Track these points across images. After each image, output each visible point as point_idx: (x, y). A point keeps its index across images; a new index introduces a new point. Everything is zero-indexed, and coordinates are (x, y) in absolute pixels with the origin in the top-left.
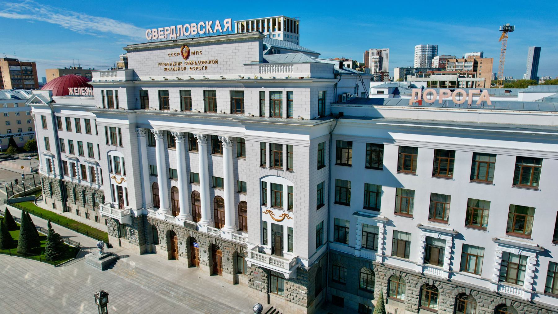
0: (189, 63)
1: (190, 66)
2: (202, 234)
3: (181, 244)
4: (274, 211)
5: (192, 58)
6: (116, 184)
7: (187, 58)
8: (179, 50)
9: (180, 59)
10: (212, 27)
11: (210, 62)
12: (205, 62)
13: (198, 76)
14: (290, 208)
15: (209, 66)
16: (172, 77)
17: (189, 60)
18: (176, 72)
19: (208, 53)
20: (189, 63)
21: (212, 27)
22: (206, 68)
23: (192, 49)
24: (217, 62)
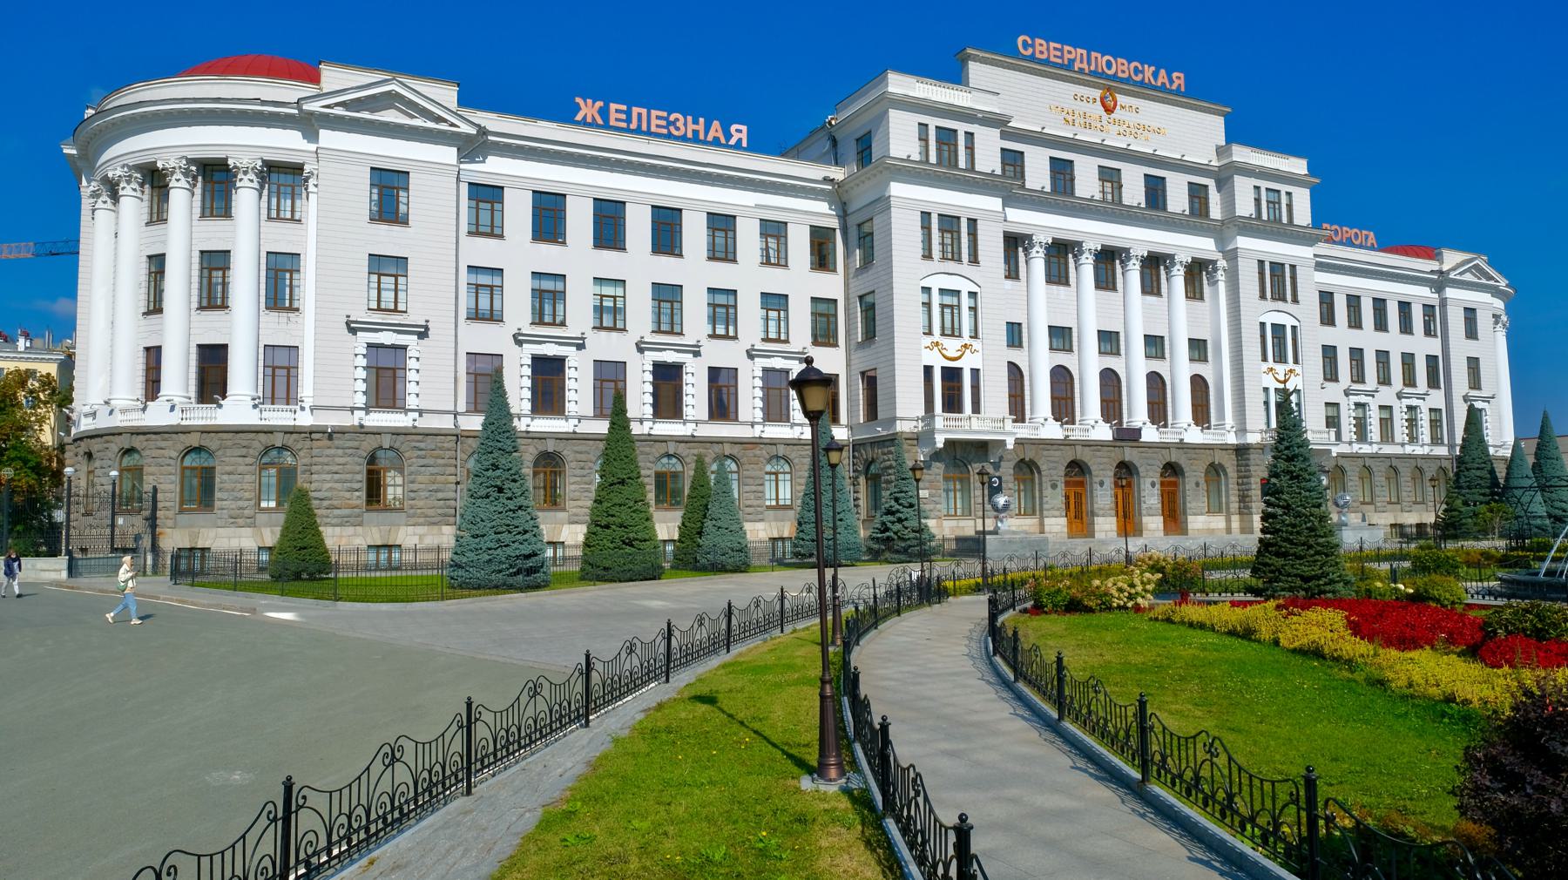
1: (1116, 128)
6: (938, 363)
8: (1097, 93)
10: (1155, 75)
21: (1155, 75)
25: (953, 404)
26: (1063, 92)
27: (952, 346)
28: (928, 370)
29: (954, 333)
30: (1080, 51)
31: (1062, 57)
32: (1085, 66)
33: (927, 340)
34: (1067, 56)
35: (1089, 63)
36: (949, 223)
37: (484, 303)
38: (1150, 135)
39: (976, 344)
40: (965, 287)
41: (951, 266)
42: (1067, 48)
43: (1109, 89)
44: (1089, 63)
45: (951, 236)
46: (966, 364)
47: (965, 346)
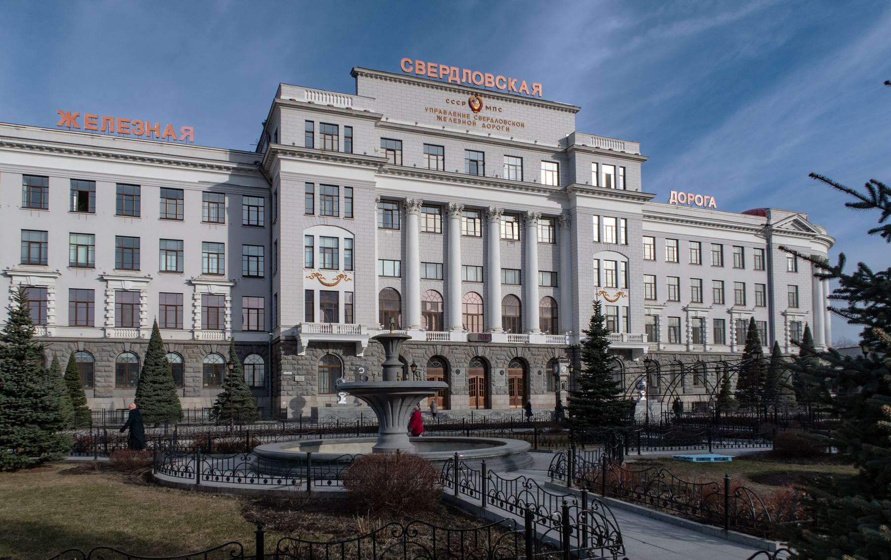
0: (480, 118)
1: (482, 122)
2: (501, 346)
3: (458, 372)
4: (608, 291)
5: (483, 113)
7: (479, 110)
8: (466, 98)
9: (468, 110)
10: (518, 85)
11: (513, 124)
12: (505, 122)
13: (495, 135)
14: (627, 286)
15: (511, 127)
16: (451, 128)
17: (480, 114)
18: (458, 125)
19: (511, 111)
20: (480, 118)
22: (508, 129)
23: (486, 101)
24: (523, 125)
25: (331, 314)
26: (438, 98)
27: (330, 276)
28: (310, 294)
29: (334, 267)
30: (453, 68)
31: (438, 73)
32: (457, 79)
33: (309, 272)
34: (441, 72)
35: (461, 77)
36: (330, 191)
37: (172, 259)
38: (511, 127)
39: (350, 275)
40: (342, 235)
41: (331, 220)
42: (441, 67)
43: (476, 95)
44: (461, 77)
45: (329, 199)
46: (344, 288)
47: (341, 276)
